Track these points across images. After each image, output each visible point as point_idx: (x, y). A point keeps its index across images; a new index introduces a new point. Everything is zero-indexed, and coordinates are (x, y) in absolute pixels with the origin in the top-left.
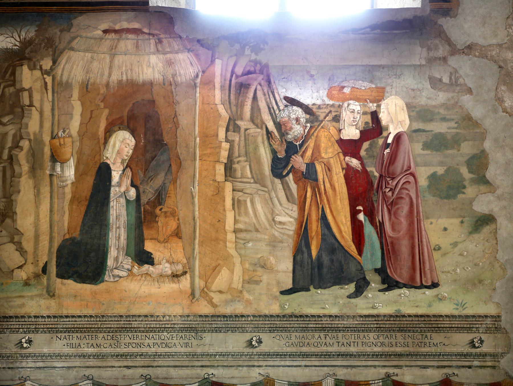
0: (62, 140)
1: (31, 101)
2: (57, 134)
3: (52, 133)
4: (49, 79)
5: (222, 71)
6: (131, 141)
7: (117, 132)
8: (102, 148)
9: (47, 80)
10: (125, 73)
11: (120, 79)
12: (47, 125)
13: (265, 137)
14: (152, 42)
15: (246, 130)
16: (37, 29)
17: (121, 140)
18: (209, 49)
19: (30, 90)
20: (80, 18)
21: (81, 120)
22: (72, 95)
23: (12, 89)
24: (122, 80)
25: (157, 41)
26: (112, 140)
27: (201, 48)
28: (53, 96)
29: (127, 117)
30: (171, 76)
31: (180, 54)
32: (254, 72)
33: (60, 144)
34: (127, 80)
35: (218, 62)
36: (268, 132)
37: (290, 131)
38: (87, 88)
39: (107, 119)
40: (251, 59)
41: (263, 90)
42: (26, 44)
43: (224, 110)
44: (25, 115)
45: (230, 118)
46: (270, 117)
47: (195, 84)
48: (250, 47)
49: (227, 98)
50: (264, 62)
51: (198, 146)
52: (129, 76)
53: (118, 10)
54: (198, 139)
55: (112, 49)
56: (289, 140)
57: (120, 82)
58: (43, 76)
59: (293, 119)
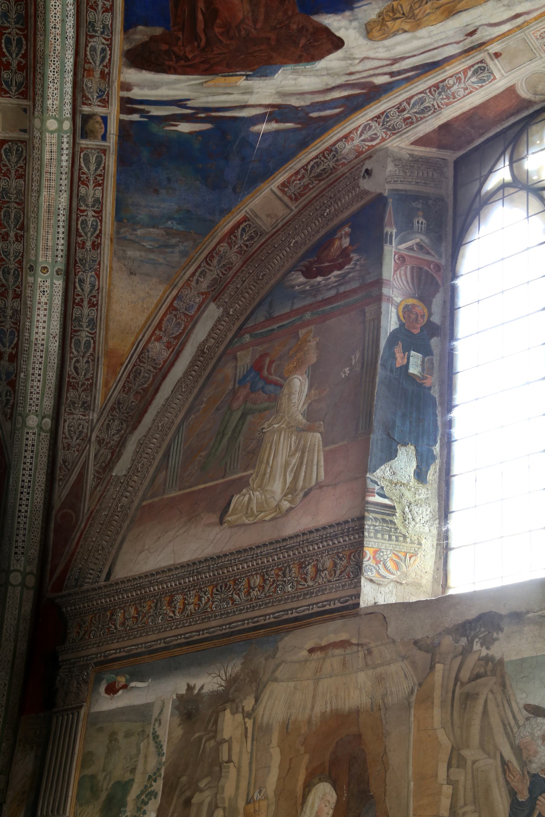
0: (257, 805)
1: (230, 756)
2: (253, 797)
3: (248, 795)
4: (249, 723)
5: (443, 680)
6: (332, 797)
7: (317, 786)
8: (299, 810)
9: (247, 725)
10: (329, 702)
11: (324, 711)
12: (244, 785)
13: (500, 770)
14: (361, 654)
15: (474, 762)
16: (243, 661)
17: (321, 796)
18: (427, 652)
19: (230, 741)
20: (286, 639)
21: (279, 773)
22: (271, 741)
23: (212, 743)
24: (326, 711)
25: (366, 652)
26: (310, 798)
27: (419, 652)
28: (252, 745)
29: (329, 762)
30: (380, 697)
31: (392, 665)
32: (485, 675)
33: (255, 810)
34: (332, 710)
35: (439, 667)
36: (505, 764)
37: (535, 756)
38: (287, 729)
39: (307, 768)
40: (481, 656)
41: (496, 699)
42: (232, 681)
43: (445, 737)
44: (223, 774)
45: (452, 746)
46: (506, 740)
47: (409, 703)
48: (480, 638)
49: (449, 718)
50: (498, 656)
51: (412, 794)
52: (334, 705)
53: (326, 620)
54: (412, 784)
55: (317, 672)
56: (533, 772)
57: (323, 714)
58: (244, 720)
59: (538, 737)
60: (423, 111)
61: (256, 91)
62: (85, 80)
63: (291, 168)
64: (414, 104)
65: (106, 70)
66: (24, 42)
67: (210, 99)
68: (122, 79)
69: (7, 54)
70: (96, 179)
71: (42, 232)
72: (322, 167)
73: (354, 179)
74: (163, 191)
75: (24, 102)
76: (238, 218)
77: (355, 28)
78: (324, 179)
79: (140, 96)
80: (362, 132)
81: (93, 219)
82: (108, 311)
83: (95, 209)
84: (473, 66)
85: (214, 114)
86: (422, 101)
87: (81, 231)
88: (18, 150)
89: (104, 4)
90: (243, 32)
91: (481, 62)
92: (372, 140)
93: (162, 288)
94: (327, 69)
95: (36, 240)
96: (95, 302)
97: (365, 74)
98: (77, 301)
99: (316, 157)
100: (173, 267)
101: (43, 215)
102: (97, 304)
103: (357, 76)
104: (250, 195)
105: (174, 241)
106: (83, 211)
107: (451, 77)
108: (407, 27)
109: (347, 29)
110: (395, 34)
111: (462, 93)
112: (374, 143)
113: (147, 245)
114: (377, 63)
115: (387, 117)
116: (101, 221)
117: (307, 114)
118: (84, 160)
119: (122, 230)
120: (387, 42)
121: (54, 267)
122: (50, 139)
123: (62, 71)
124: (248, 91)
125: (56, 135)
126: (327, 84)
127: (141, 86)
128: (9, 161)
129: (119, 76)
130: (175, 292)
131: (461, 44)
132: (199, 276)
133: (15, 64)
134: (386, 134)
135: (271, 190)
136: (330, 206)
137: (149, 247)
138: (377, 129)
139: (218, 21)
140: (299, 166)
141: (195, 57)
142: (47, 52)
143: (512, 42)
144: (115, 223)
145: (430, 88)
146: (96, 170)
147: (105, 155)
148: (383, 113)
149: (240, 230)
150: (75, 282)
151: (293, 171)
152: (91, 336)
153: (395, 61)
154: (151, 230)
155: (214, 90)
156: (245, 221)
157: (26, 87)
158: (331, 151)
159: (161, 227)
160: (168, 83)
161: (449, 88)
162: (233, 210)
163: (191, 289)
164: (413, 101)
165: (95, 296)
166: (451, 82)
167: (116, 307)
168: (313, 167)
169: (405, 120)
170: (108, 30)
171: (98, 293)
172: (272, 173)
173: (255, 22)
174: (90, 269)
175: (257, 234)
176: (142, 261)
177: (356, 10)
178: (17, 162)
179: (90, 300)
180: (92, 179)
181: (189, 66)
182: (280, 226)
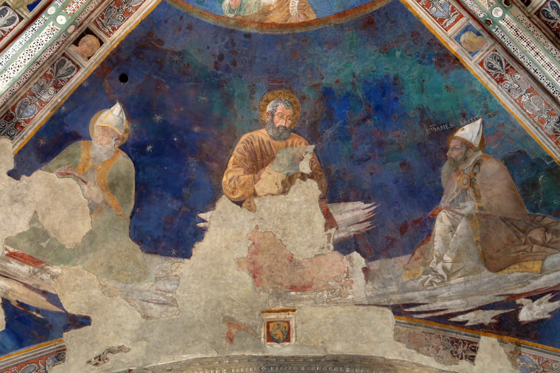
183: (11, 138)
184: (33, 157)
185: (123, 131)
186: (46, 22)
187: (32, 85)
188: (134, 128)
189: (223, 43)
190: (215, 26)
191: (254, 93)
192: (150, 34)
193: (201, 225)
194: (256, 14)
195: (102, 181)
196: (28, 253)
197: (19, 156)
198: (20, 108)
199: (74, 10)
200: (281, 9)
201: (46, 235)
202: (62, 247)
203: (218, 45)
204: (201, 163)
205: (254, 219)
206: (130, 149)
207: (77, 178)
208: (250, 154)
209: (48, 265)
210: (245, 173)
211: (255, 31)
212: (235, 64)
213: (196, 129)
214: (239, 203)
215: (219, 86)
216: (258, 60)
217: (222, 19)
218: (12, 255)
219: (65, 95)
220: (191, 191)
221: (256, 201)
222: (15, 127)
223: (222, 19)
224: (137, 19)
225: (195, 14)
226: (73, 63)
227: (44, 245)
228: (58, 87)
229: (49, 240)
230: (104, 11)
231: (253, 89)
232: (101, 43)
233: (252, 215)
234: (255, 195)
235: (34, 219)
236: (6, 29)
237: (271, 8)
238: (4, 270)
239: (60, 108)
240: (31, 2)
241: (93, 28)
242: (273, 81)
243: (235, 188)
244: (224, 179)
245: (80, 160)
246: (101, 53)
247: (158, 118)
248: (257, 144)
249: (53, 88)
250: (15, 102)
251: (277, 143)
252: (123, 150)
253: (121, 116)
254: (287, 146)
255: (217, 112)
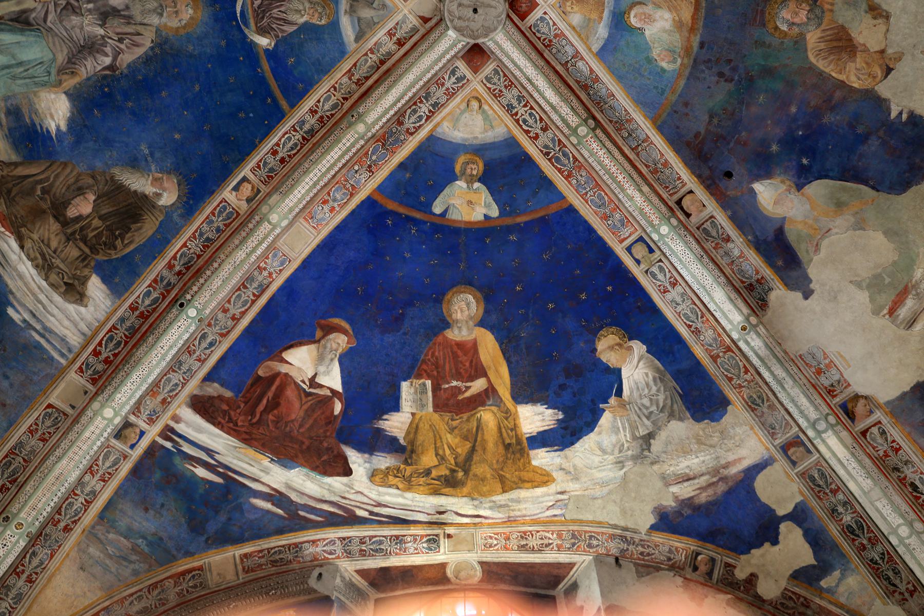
60: (376, 551)
61: (271, 473)
62: (148, 397)
63: (259, 545)
64: (374, 542)
65: (169, 400)
66: (122, 346)
67: (235, 461)
68: (177, 412)
69: (103, 346)
70: (104, 474)
71: (39, 493)
72: (281, 556)
73: (304, 577)
74: (151, 512)
75: (90, 387)
76: (196, 564)
77: (365, 468)
78: (277, 566)
79: (183, 431)
80: (327, 544)
81: (80, 505)
82: (40, 592)
83: (87, 498)
84: (429, 535)
85: (230, 474)
86: (381, 543)
87: (63, 510)
88: (57, 418)
89: (200, 355)
90: (288, 429)
91: (436, 535)
92: (331, 553)
93: (99, 594)
94: (330, 485)
95: (29, 497)
96: (34, 579)
97: (353, 503)
98: (18, 570)
99: (283, 546)
100: (120, 580)
101: (51, 478)
102: (34, 582)
103: (347, 502)
104: (216, 551)
105: (134, 558)
106: (76, 495)
107: (411, 536)
108: (400, 486)
109: (359, 466)
110: (390, 486)
111: (412, 551)
112: (330, 557)
113: (110, 550)
114: (365, 500)
115: (350, 542)
116: (86, 510)
117: (298, 510)
118: (105, 455)
119: (98, 527)
120: (381, 489)
121: (29, 527)
122: (99, 422)
123: (144, 380)
124: (266, 471)
125: (106, 422)
126: (324, 496)
127: (188, 424)
128: (43, 422)
129: (177, 409)
130: (107, 604)
131: (430, 516)
132: (136, 599)
133: (104, 356)
134: (343, 554)
135: (234, 555)
136: (275, 589)
137: (111, 552)
138: (338, 548)
139: (275, 412)
140: (266, 546)
141: (243, 426)
142: (143, 360)
143: (464, 532)
144: (96, 518)
145: (392, 536)
146: (109, 467)
147: (124, 460)
148: (348, 538)
149: (190, 575)
150: (28, 552)
151: (259, 548)
152: (10, 609)
153: (379, 505)
154: (122, 539)
155: (242, 457)
156: (199, 570)
157: (100, 377)
158: (297, 547)
159: (132, 541)
160: (210, 434)
161: (405, 543)
162: (196, 556)
163: (122, 606)
164: (374, 539)
165: (36, 574)
166: (409, 539)
167: (49, 592)
168: (276, 552)
169: (361, 550)
170: (191, 373)
171: (41, 572)
172: (243, 542)
173: (301, 426)
174: (50, 546)
175: (201, 586)
176: (97, 561)
177: (374, 456)
178: (49, 427)
179: (31, 575)
180: (101, 473)
181: (235, 430)
182: (223, 587)
183: (770, 289)
184: (794, 274)
185: (782, 185)
186: (665, 243)
187: (724, 263)
188: (781, 173)
189: (706, 72)
190: (688, 79)
191: (764, 42)
192: (688, 144)
193: (904, 117)
194: (680, 35)
195: (832, 214)
196: (893, 297)
197: (790, 286)
198: (743, 276)
199: (657, 217)
200: (679, 8)
201: (877, 277)
202: (895, 263)
203: (708, 77)
204: (832, 109)
205: (913, 55)
206: (802, 180)
207: (823, 237)
208: (832, 53)
209: (911, 280)
210: (854, 61)
211: (698, 36)
212: (730, 61)
213: (793, 109)
214: (889, 71)
215: (751, 79)
216: (729, 36)
217: (681, 71)
218: (892, 312)
219: (737, 234)
220: (862, 124)
221: (890, 51)
222: (761, 284)
223: (681, 71)
224: (672, 155)
225: (674, 98)
226: (706, 221)
227: (887, 280)
228: (728, 239)
229: (884, 275)
230: (661, 185)
231: (760, 43)
232: (691, 192)
233: (907, 59)
234: (882, 52)
235: (859, 285)
236: (668, 275)
237: (677, 18)
238: (906, 322)
239: (749, 240)
240: (647, 249)
241: (676, 197)
242: (755, 20)
243: (870, 75)
244: (856, 85)
245: (805, 231)
246: (701, 193)
247: (775, 148)
248: (823, 44)
249: (729, 244)
250: (737, 280)
251: (825, 21)
252: (802, 188)
253: (766, 184)
254: (831, 11)
255: (779, 86)
